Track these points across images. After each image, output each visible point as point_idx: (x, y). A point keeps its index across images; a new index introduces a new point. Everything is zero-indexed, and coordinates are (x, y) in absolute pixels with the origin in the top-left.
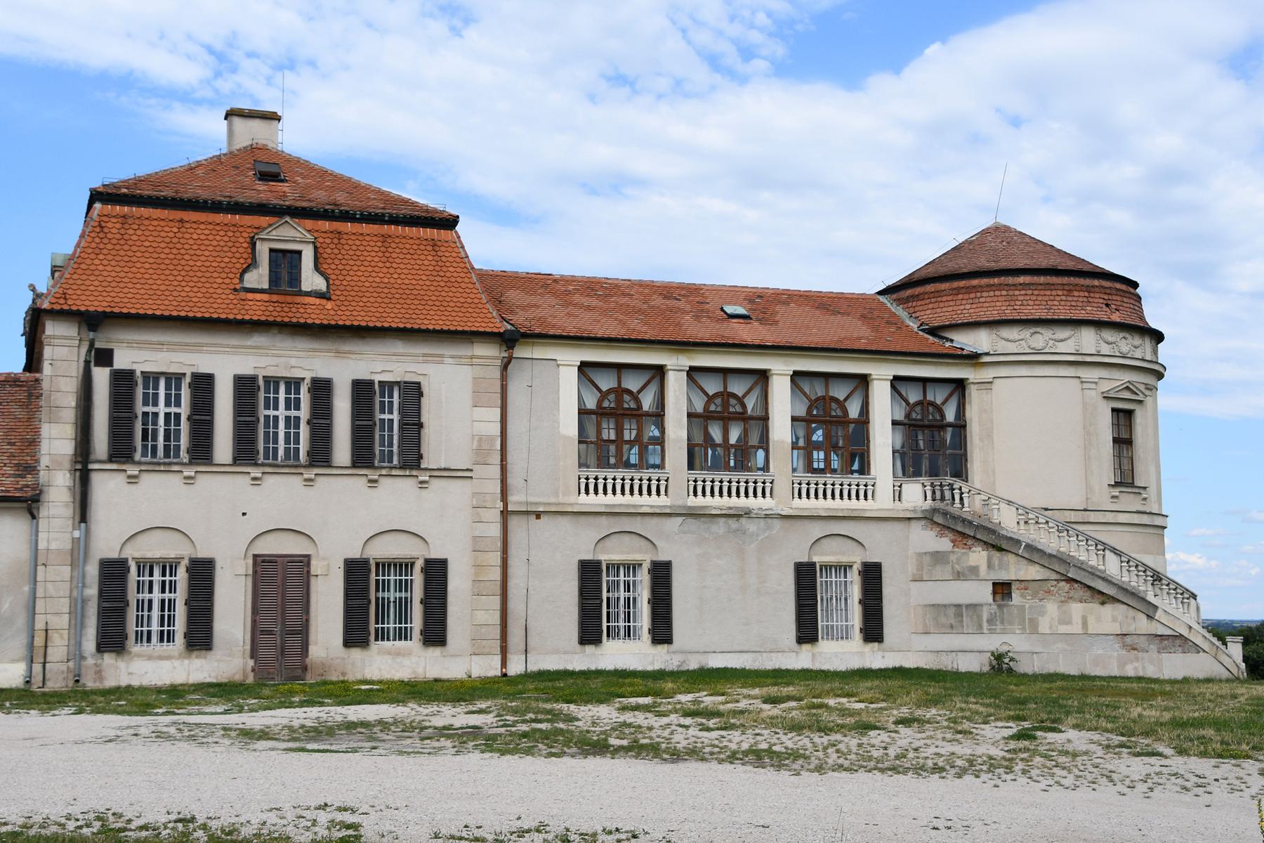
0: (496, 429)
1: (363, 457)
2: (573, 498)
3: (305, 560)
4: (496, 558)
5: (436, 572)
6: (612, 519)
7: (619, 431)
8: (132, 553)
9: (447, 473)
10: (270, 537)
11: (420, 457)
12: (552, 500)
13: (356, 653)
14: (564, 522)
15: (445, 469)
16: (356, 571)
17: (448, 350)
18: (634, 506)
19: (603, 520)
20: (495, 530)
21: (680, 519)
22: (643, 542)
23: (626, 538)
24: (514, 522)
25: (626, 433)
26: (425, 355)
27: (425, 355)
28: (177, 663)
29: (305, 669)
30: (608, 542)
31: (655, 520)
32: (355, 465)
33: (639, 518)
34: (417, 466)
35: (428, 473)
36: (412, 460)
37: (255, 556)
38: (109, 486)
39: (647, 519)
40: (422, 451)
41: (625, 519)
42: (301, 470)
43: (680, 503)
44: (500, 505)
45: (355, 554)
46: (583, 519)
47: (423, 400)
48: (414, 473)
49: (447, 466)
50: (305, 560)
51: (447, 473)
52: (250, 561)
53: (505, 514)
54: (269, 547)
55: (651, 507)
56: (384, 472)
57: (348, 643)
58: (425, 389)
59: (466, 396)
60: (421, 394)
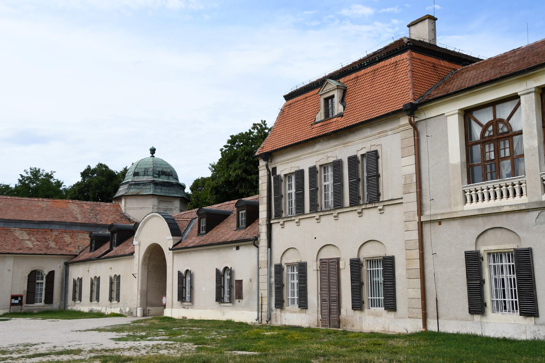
0: (412, 169)
1: (355, 201)
2: (460, 207)
3: (338, 260)
4: (416, 254)
5: (388, 264)
6: (485, 219)
7: (497, 152)
8: (285, 261)
9: (395, 202)
10: (325, 250)
11: (379, 195)
12: (449, 210)
13: (358, 313)
14: (455, 224)
15: (391, 200)
16: (356, 265)
17: (388, 127)
18: (498, 207)
19: (480, 220)
20: (415, 235)
21: (536, 213)
22: (511, 235)
23: (498, 233)
24: (427, 229)
25: (502, 152)
26: (379, 133)
27: (379, 133)
28: (298, 315)
29: (339, 322)
30: (486, 237)
31: (516, 216)
32: (352, 205)
33: (504, 216)
34: (378, 201)
35: (383, 204)
36: (375, 197)
37: (321, 260)
38: (276, 229)
39: (511, 216)
40: (381, 191)
41: (494, 218)
42: (332, 212)
43: (536, 199)
44: (417, 218)
45: (355, 256)
46: (467, 221)
47: (380, 161)
48: (376, 205)
49: (392, 198)
50: (338, 260)
51: (395, 202)
52: (319, 263)
53: (421, 224)
54: (327, 254)
55: (510, 206)
56: (364, 207)
57: (354, 308)
58: (380, 154)
59: (399, 152)
60: (377, 157)
